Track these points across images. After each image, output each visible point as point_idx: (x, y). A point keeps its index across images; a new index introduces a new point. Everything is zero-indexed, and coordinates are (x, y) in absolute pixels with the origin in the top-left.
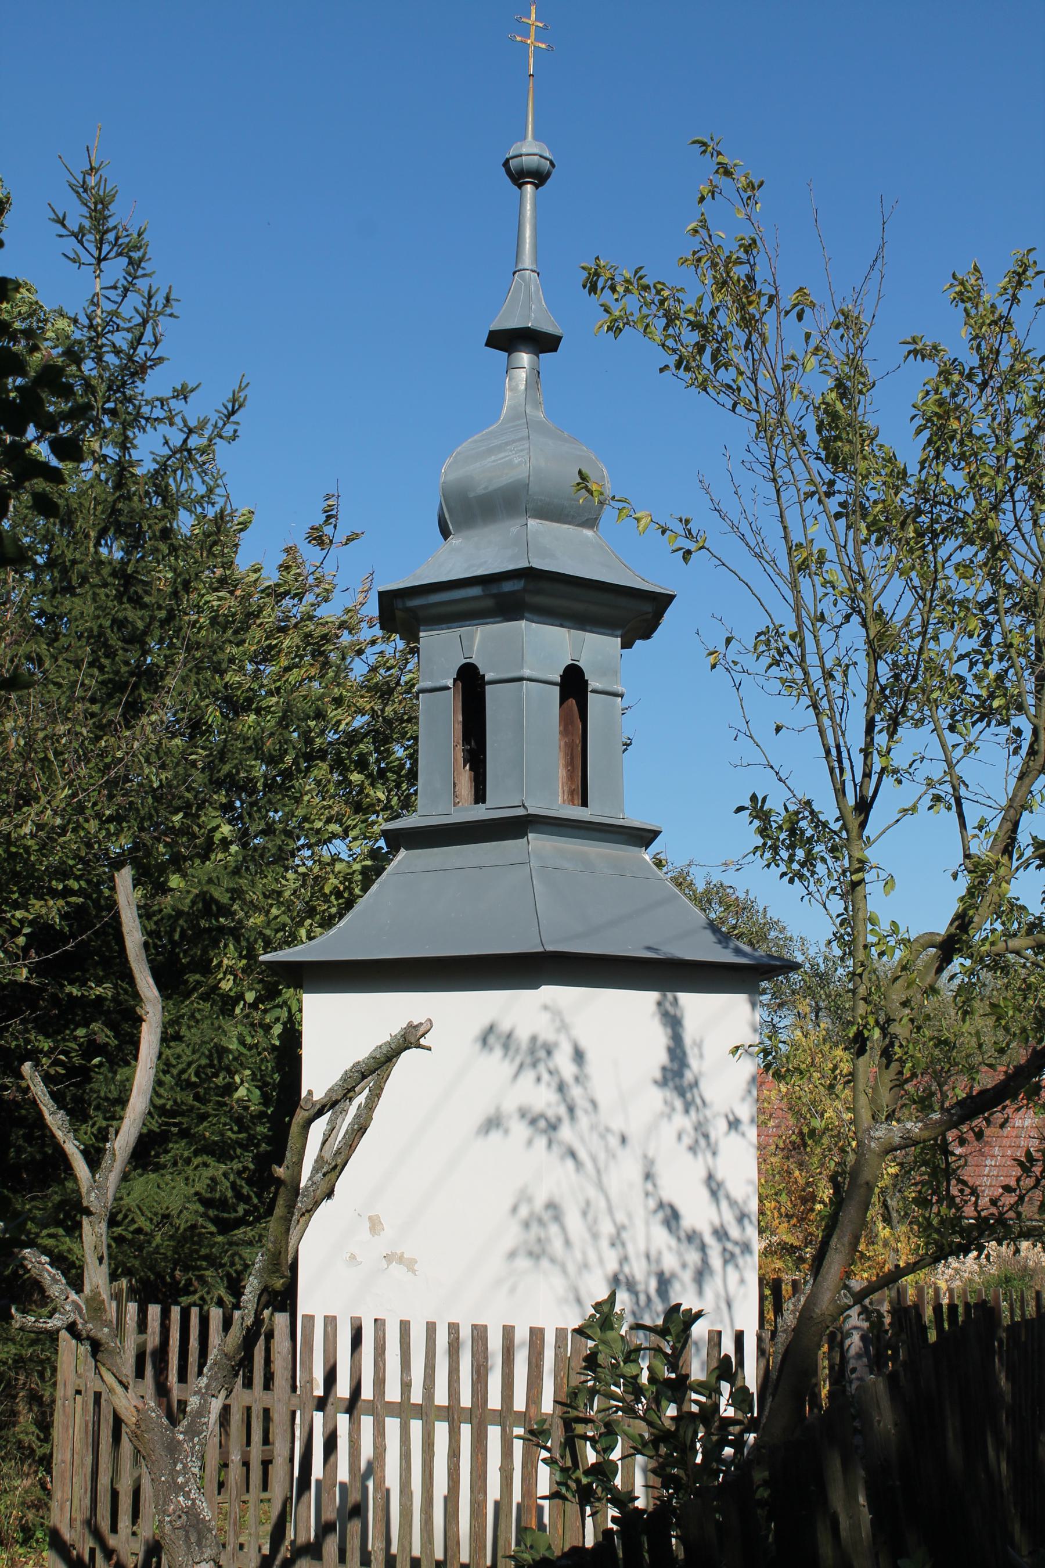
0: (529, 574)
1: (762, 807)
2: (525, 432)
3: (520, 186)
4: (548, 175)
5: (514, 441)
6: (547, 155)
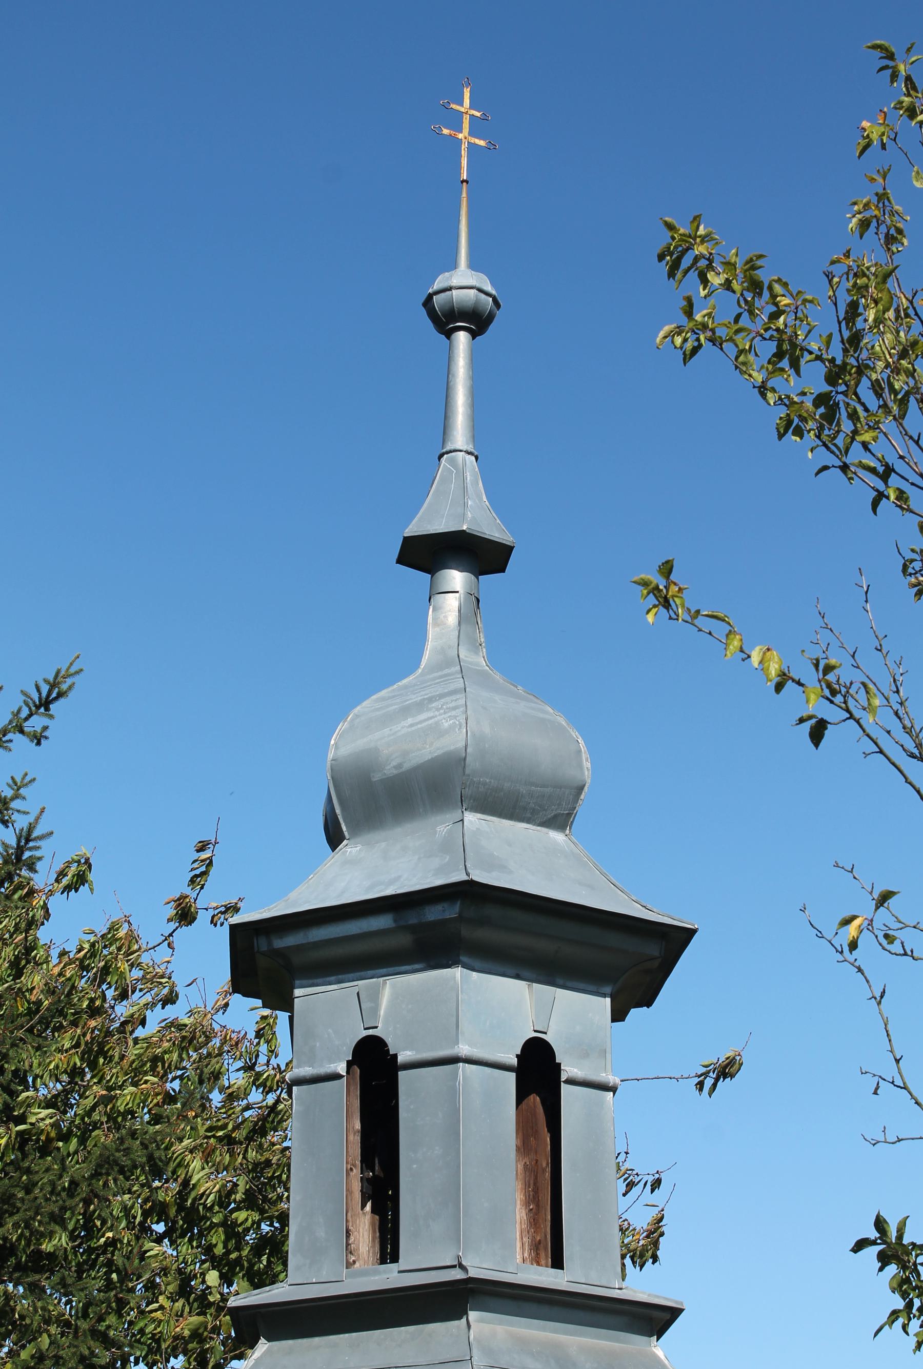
0: (468, 892)
1: (900, 1237)
2: (460, 684)
3: (448, 334)
4: (490, 318)
5: (442, 696)
6: (489, 288)
